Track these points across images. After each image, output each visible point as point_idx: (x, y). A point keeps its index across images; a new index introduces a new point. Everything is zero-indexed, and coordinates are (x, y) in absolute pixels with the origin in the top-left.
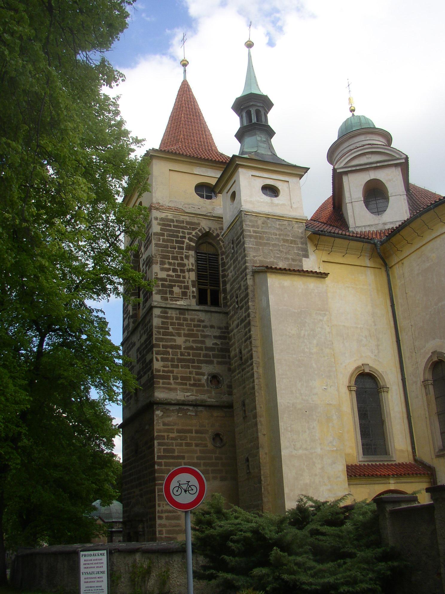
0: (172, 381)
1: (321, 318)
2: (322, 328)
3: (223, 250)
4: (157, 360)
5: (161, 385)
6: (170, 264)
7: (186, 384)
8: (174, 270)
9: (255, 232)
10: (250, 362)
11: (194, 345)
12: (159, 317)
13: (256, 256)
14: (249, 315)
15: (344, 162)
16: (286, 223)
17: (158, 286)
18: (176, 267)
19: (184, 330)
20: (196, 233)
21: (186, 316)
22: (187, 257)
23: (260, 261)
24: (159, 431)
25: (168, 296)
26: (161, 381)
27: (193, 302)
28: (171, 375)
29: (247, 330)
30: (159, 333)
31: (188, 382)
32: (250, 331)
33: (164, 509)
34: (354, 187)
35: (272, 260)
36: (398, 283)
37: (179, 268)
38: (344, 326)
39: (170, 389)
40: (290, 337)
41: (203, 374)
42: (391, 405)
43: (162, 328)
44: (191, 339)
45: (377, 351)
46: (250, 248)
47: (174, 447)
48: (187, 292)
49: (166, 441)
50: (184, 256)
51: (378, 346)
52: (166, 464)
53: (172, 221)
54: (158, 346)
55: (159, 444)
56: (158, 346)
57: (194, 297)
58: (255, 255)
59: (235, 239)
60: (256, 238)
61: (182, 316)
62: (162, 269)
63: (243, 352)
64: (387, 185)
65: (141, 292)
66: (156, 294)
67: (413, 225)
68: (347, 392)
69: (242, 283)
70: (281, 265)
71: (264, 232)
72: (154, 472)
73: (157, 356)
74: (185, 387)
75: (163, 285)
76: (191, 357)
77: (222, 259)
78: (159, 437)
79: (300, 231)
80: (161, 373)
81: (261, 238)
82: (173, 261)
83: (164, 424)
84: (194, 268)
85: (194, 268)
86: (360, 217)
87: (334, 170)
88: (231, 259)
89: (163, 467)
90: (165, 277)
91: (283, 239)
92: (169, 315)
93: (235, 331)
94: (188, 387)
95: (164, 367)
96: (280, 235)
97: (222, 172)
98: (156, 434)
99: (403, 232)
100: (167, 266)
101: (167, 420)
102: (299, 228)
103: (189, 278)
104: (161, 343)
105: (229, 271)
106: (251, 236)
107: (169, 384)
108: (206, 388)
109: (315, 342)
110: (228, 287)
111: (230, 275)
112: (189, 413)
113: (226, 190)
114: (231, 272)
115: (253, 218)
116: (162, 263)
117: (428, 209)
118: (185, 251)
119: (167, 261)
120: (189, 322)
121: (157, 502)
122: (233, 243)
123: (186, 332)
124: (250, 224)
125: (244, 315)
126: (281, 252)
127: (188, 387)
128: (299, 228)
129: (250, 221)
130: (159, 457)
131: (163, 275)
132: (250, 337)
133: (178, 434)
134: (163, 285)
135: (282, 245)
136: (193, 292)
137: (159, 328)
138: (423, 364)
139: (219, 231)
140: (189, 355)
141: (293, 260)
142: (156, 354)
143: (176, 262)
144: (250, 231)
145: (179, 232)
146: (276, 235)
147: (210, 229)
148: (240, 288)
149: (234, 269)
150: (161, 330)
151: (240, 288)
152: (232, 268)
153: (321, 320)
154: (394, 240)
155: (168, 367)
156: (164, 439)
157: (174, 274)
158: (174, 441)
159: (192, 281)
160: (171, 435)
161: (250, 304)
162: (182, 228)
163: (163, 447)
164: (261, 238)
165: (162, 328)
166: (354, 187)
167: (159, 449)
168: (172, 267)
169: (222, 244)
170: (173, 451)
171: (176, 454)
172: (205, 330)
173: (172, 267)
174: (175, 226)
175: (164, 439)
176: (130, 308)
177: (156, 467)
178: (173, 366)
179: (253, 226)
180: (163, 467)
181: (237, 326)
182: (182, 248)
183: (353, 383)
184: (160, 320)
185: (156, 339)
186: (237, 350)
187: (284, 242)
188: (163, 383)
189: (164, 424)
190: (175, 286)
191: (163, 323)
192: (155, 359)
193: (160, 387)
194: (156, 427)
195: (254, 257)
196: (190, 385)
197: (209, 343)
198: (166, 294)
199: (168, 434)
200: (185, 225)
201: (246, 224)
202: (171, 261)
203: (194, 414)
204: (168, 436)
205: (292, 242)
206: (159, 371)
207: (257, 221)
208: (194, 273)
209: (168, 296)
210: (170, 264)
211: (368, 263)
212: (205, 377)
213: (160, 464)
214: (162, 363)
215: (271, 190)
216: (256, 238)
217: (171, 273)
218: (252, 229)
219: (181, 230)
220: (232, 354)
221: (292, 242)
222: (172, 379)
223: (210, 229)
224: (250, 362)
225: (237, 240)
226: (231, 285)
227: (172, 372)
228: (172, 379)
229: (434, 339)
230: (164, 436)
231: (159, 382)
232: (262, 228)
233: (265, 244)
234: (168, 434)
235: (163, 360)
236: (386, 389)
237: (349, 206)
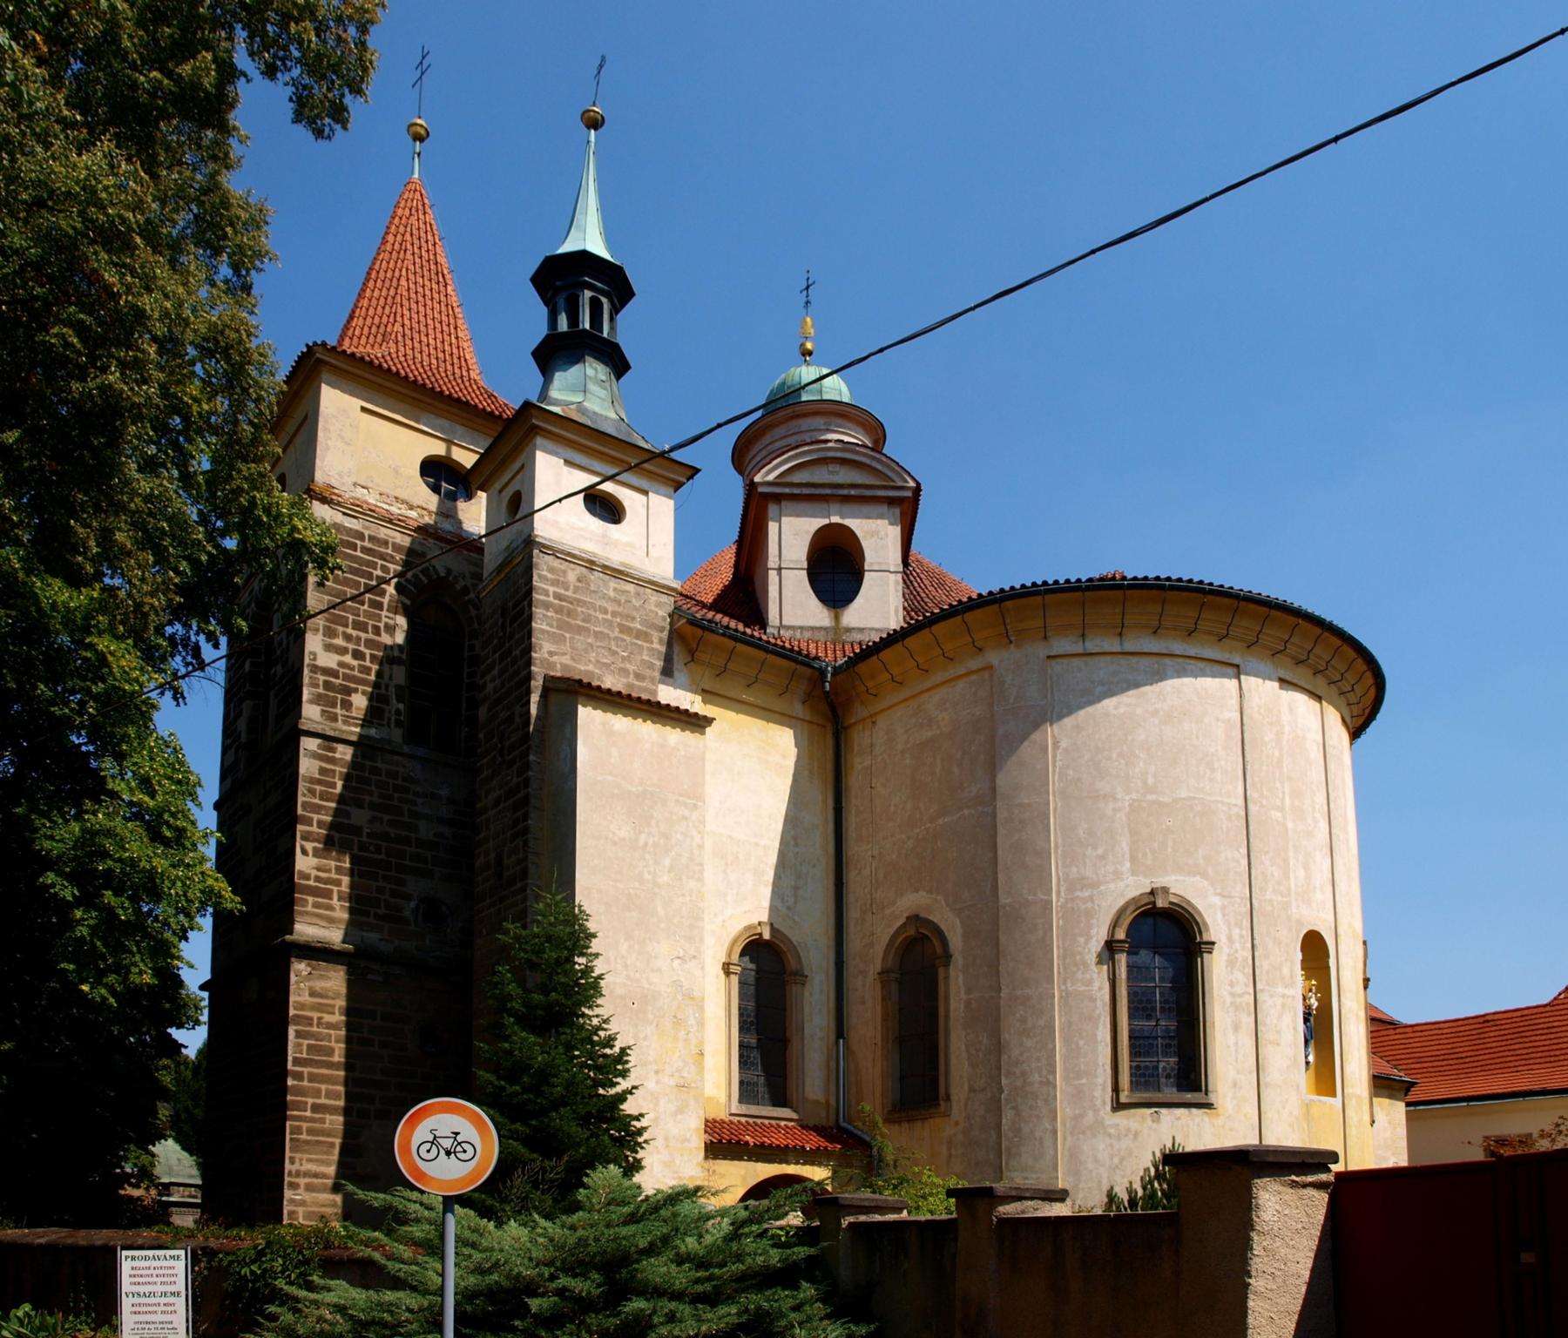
1: (687, 813)
2: (684, 834)
3: (476, 626)
4: (304, 852)
5: (309, 908)
6: (348, 638)
7: (368, 915)
8: (358, 655)
9: (557, 596)
10: (519, 885)
11: (392, 832)
12: (315, 756)
13: (556, 654)
14: (526, 783)
15: (777, 472)
17: (317, 686)
18: (362, 648)
19: (371, 794)
20: (414, 576)
21: (379, 765)
22: (391, 629)
23: (564, 666)
24: (302, 1006)
25: (338, 711)
26: (310, 899)
27: (397, 735)
28: (335, 889)
29: (519, 814)
30: (312, 792)
32: (525, 817)
33: (303, 1168)
34: (791, 537)
35: (591, 668)
36: (858, 765)
37: (368, 652)
38: (731, 837)
40: (615, 843)
41: (408, 898)
42: (807, 1010)
43: (320, 782)
44: (387, 817)
45: (791, 900)
46: (543, 631)
47: (333, 1044)
48: (383, 711)
50: (382, 625)
51: (796, 888)
52: (312, 1078)
53: (361, 536)
54: (309, 822)
55: (299, 1034)
56: (309, 822)
57: (399, 724)
58: (553, 652)
59: (510, 604)
61: (368, 763)
62: (329, 648)
63: (506, 861)
64: (864, 544)
65: (272, 694)
66: (311, 702)
67: (910, 642)
68: (722, 976)
69: (517, 709)
70: (610, 682)
71: (579, 601)
72: (284, 1089)
74: (364, 919)
75: (327, 685)
76: (383, 856)
77: (472, 648)
78: (299, 1019)
79: (661, 613)
80: (311, 883)
81: (569, 613)
82: (354, 633)
83: (313, 994)
84: (404, 656)
85: (404, 656)
86: (793, 605)
87: (751, 487)
88: (495, 652)
89: (305, 1083)
90: (334, 666)
91: (620, 625)
92: (337, 755)
93: (491, 813)
94: (372, 920)
95: (318, 869)
96: (614, 614)
97: (487, 442)
98: (292, 1012)
99: (886, 655)
100: (339, 641)
101: (319, 985)
103: (391, 678)
104: (316, 817)
105: (488, 677)
106: (547, 606)
108: (412, 927)
109: (667, 862)
110: (483, 712)
111: (490, 686)
113: (498, 486)
114: (493, 680)
116: (330, 633)
117: (946, 615)
118: (384, 613)
119: (341, 629)
120: (383, 778)
121: (288, 1154)
122: (503, 615)
123: (375, 799)
125: (515, 780)
126: (614, 653)
127: (372, 920)
129: (551, 570)
130: (297, 1061)
131: (329, 660)
132: (526, 831)
134: (327, 685)
135: (616, 639)
136: (398, 712)
137: (312, 781)
138: (886, 939)
139: (469, 582)
140: (378, 850)
141: (638, 676)
142: (303, 838)
143: (363, 635)
145: (374, 565)
146: (606, 612)
147: (449, 571)
148: (510, 720)
149: (502, 672)
150: (318, 788)
151: (510, 720)
152: (495, 672)
153: (685, 818)
154: (862, 668)
155: (329, 871)
156: (311, 1025)
157: (355, 663)
159: (398, 687)
161: (532, 758)
162: (382, 557)
163: (306, 1042)
164: (569, 613)
165: (320, 782)
166: (791, 537)
167: (299, 1045)
168: (351, 646)
169: (473, 612)
170: (331, 1051)
172: (420, 801)
173: (351, 646)
174: (365, 550)
175: (311, 1025)
176: (242, 725)
177: (290, 1082)
179: (555, 583)
180: (305, 1083)
181: (497, 803)
182: (379, 606)
183: (735, 958)
184: (317, 764)
185: (305, 805)
186: (493, 855)
187: (621, 632)
188: (316, 905)
190: (356, 691)
191: (322, 771)
192: (298, 850)
193: (307, 913)
194: (292, 999)
195: (551, 653)
196: (377, 916)
197: (425, 831)
198: (334, 705)
200: (389, 551)
201: (540, 576)
202: (350, 631)
204: (320, 1019)
205: (640, 635)
206: (307, 877)
207: (565, 572)
208: (403, 668)
209: (338, 711)
210: (348, 638)
211: (799, 709)
212: (412, 904)
213: (299, 1076)
214: (316, 860)
215: (606, 508)
216: (559, 610)
217: (348, 659)
218: (551, 589)
219: (380, 562)
220: (480, 862)
221: (640, 635)
222: (335, 897)
223: (449, 571)
224: (519, 885)
225: (516, 605)
226: (489, 710)
228: (335, 897)
229: (917, 890)
230: (311, 1019)
232: (576, 590)
236: (801, 977)
237: (773, 575)
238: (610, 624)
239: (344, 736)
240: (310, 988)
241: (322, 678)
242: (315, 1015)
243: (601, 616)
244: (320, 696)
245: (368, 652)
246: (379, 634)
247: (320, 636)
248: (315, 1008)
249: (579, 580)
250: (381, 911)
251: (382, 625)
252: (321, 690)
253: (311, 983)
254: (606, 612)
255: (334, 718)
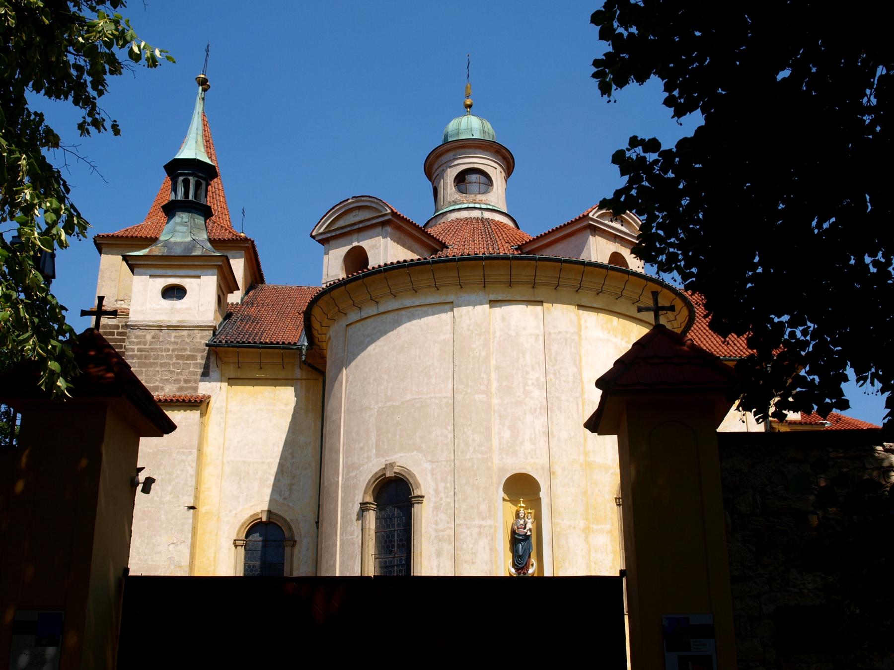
9: (140, 350)
16: (185, 333)
60: (140, 357)
81: (146, 357)
96: (173, 350)
102: (202, 337)
106: (132, 357)
115: (139, 333)
124: (136, 340)
128: (202, 337)
144: (133, 350)
164: (146, 357)
179: (139, 343)
205: (190, 357)
218: (136, 347)
221: (190, 357)
233: (152, 364)
238: (170, 357)
243: (164, 354)
249: (153, 338)
254: (168, 350)
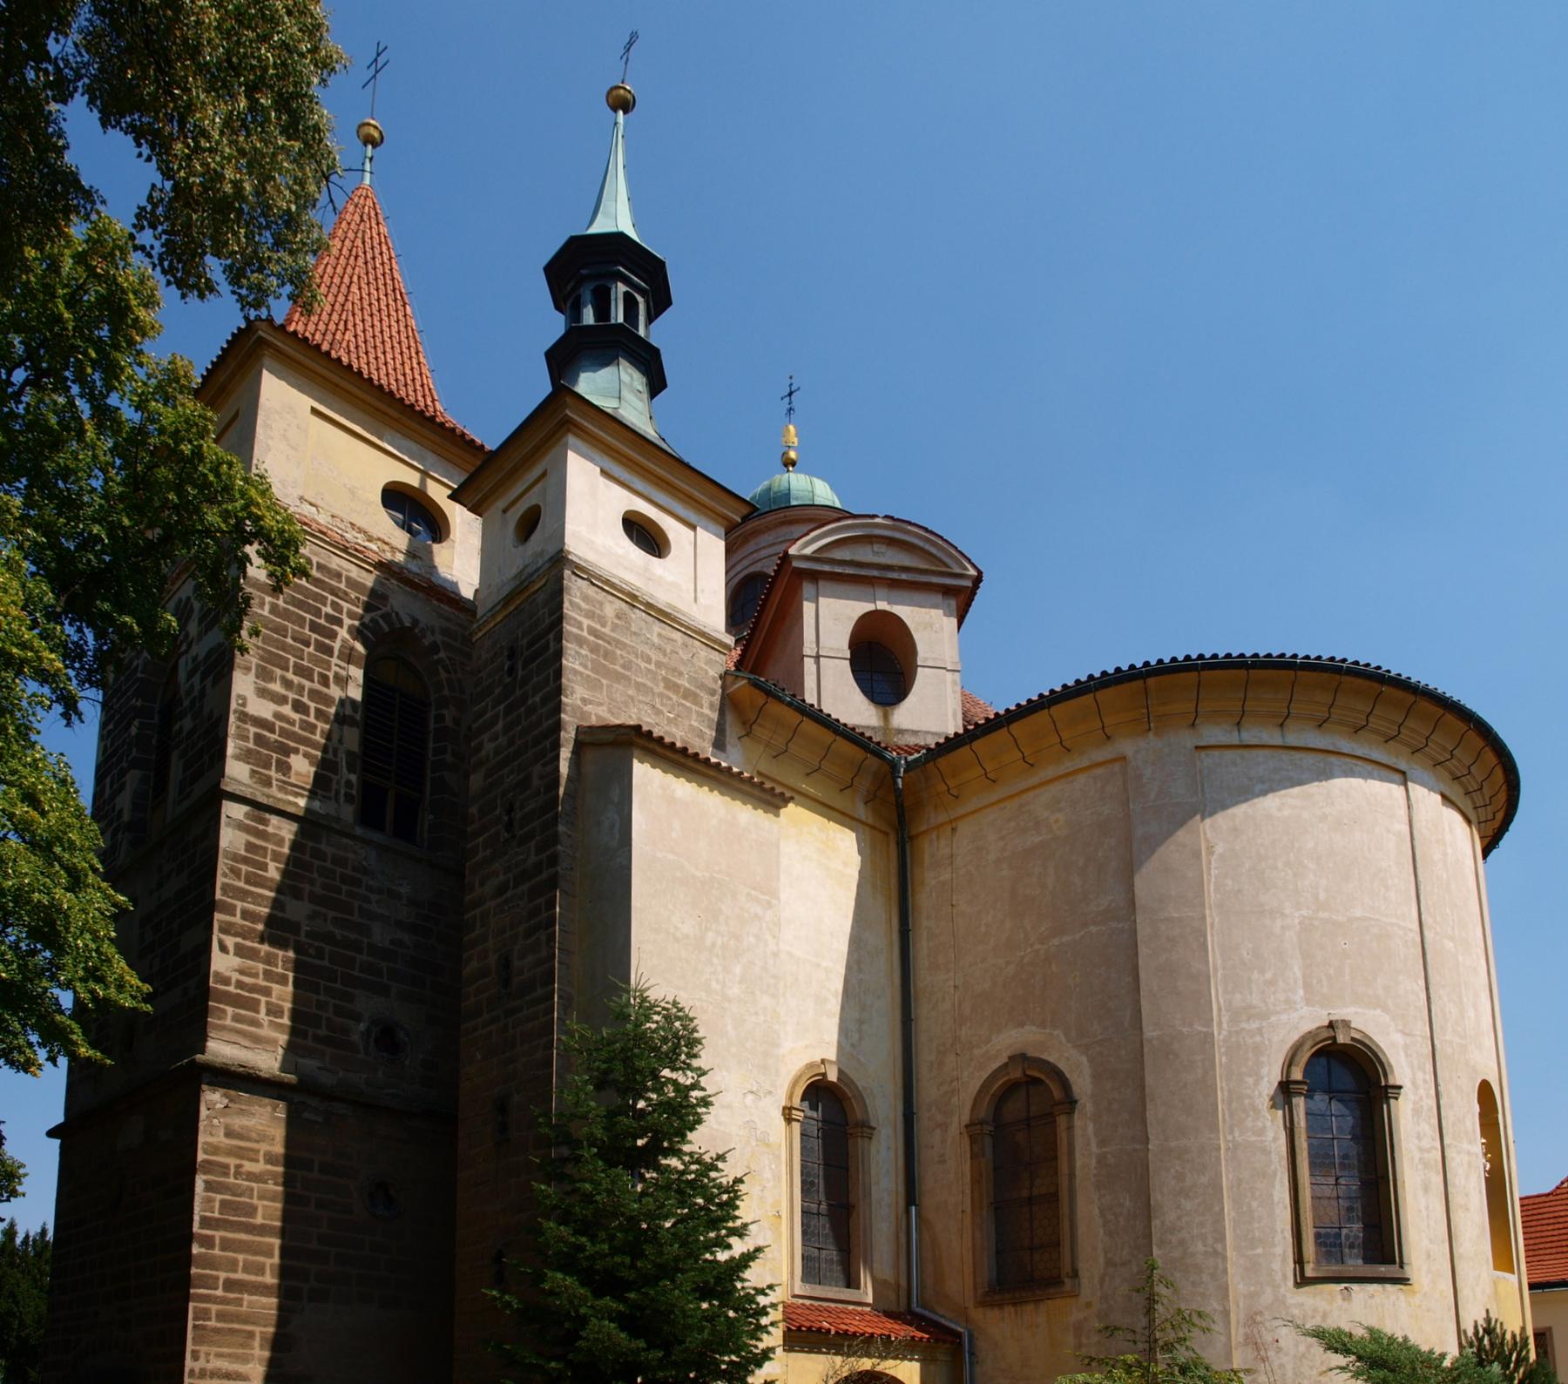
0: (262, 1015)
4: (223, 949)
5: (228, 1022)
6: (287, 684)
8: (299, 707)
12: (241, 826)
17: (246, 738)
18: (305, 700)
21: (323, 847)
24: (215, 1149)
25: (273, 773)
26: (230, 1010)
27: (348, 812)
28: (263, 999)
30: (236, 873)
31: (311, 1031)
33: (210, 1366)
37: (312, 705)
39: (257, 1040)
41: (357, 1018)
43: (245, 861)
44: (331, 914)
47: (255, 1201)
49: (232, 1180)
50: (331, 675)
52: (227, 1245)
54: (230, 910)
55: (209, 1186)
56: (230, 910)
57: (349, 798)
62: (263, 693)
66: (237, 758)
73: (223, 937)
75: (259, 739)
76: (326, 963)
78: (210, 1166)
80: (231, 989)
82: (296, 679)
83: (229, 1134)
84: (358, 717)
85: (358, 717)
89: (217, 1252)
90: (270, 717)
92: (270, 829)
94: (310, 1042)
95: (242, 972)
98: (201, 1156)
100: (276, 687)
101: (238, 1122)
103: (340, 741)
104: (239, 904)
107: (256, 1023)
112: (306, 1115)
116: (264, 674)
118: (334, 660)
119: (279, 672)
120: (328, 865)
121: (190, 1346)
123: (318, 890)
127: (310, 1042)
130: (205, 1222)
131: (262, 709)
133: (269, 1167)
134: (259, 739)
136: (349, 784)
137: (236, 858)
142: (222, 930)
143: (307, 684)
150: (244, 868)
155: (256, 975)
156: (227, 1175)
157: (296, 716)
158: (254, 1185)
159: (349, 753)
160: (249, 1166)
163: (219, 1197)
167: (210, 1200)
168: (291, 696)
171: (259, 1220)
172: (374, 897)
173: (291, 696)
175: (227, 1175)
177: (196, 1249)
178: (268, 975)
180: (217, 1252)
182: (329, 651)
185: (225, 887)
188: (236, 1018)
189: (229, 1134)
190: (296, 751)
191: (250, 847)
193: (224, 1028)
194: (202, 1139)
196: (316, 1038)
198: (267, 766)
199: (238, 1162)
202: (290, 676)
203: (320, 1119)
204: (238, 1167)
206: (227, 981)
209: (273, 773)
210: (287, 684)
212: (362, 1026)
213: (208, 1242)
217: (287, 710)
219: (330, 597)
222: (263, 1010)
227: (267, 992)
228: (263, 1010)
230: (227, 1166)
231: (224, 1011)
234: (238, 1162)
235: (240, 951)
239: (281, 806)
240: (227, 1127)
241: (253, 730)
242: (232, 1162)
244: (249, 751)
245: (312, 705)
246: (327, 685)
247: (251, 677)
248: (231, 1152)
250: (323, 1032)
251: (331, 675)
252: (251, 745)
253: (228, 1120)
255: (267, 782)
